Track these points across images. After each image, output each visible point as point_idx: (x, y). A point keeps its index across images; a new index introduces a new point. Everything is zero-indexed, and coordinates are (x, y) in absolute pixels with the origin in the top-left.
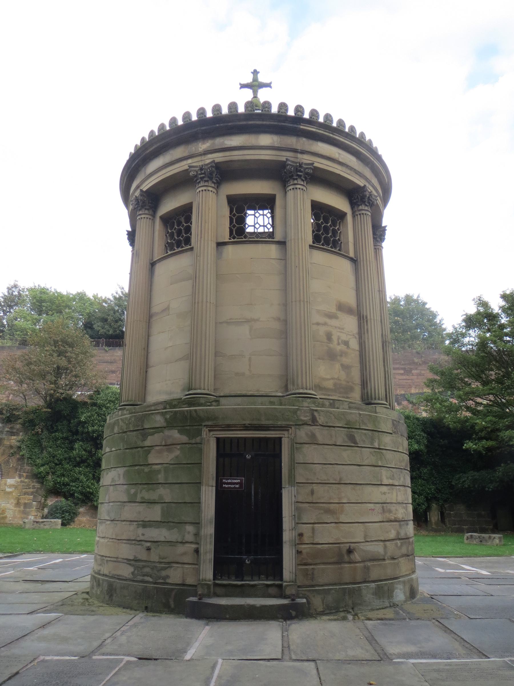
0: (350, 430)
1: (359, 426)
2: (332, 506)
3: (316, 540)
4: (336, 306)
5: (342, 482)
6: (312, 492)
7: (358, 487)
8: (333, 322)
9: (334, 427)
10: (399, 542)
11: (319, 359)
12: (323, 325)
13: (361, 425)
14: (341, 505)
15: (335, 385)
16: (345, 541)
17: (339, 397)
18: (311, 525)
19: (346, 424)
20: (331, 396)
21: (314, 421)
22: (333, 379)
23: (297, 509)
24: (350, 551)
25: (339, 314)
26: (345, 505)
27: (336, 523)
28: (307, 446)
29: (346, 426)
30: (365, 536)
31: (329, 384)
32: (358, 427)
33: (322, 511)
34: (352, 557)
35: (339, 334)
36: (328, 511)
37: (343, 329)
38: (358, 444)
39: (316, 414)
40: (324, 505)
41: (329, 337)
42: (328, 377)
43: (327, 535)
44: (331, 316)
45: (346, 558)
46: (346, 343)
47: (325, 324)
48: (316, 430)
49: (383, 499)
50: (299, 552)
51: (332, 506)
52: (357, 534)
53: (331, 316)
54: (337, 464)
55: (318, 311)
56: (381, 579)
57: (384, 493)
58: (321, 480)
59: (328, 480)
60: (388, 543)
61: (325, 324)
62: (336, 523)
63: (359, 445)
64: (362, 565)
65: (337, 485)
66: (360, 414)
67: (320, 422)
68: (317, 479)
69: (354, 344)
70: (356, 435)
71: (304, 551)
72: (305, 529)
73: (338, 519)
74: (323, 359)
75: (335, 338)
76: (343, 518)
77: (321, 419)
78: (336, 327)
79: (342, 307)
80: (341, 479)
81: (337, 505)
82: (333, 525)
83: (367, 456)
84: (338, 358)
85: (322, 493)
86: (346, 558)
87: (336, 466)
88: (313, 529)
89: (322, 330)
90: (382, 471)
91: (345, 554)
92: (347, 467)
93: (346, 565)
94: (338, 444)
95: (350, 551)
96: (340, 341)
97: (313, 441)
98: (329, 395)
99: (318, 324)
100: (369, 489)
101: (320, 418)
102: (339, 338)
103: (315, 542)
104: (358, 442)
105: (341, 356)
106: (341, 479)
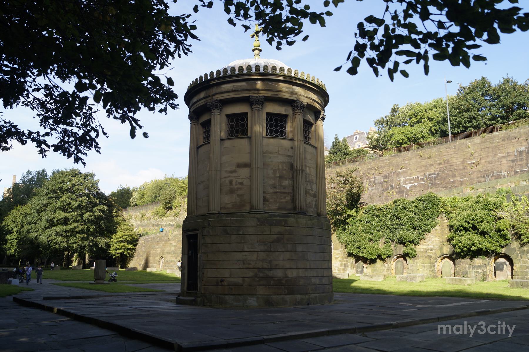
8: (234, 174)
24: (222, 281)
25: (238, 169)
31: (230, 206)
34: (223, 283)
41: (231, 182)
44: (232, 172)
45: (220, 284)
46: (241, 183)
47: (229, 177)
52: (226, 274)
53: (232, 172)
55: (226, 171)
57: (246, 255)
60: (246, 279)
61: (229, 177)
75: (234, 182)
79: (239, 166)
86: (220, 284)
89: (227, 180)
93: (220, 287)
95: (222, 281)
99: (225, 178)
102: (236, 181)
105: (237, 190)
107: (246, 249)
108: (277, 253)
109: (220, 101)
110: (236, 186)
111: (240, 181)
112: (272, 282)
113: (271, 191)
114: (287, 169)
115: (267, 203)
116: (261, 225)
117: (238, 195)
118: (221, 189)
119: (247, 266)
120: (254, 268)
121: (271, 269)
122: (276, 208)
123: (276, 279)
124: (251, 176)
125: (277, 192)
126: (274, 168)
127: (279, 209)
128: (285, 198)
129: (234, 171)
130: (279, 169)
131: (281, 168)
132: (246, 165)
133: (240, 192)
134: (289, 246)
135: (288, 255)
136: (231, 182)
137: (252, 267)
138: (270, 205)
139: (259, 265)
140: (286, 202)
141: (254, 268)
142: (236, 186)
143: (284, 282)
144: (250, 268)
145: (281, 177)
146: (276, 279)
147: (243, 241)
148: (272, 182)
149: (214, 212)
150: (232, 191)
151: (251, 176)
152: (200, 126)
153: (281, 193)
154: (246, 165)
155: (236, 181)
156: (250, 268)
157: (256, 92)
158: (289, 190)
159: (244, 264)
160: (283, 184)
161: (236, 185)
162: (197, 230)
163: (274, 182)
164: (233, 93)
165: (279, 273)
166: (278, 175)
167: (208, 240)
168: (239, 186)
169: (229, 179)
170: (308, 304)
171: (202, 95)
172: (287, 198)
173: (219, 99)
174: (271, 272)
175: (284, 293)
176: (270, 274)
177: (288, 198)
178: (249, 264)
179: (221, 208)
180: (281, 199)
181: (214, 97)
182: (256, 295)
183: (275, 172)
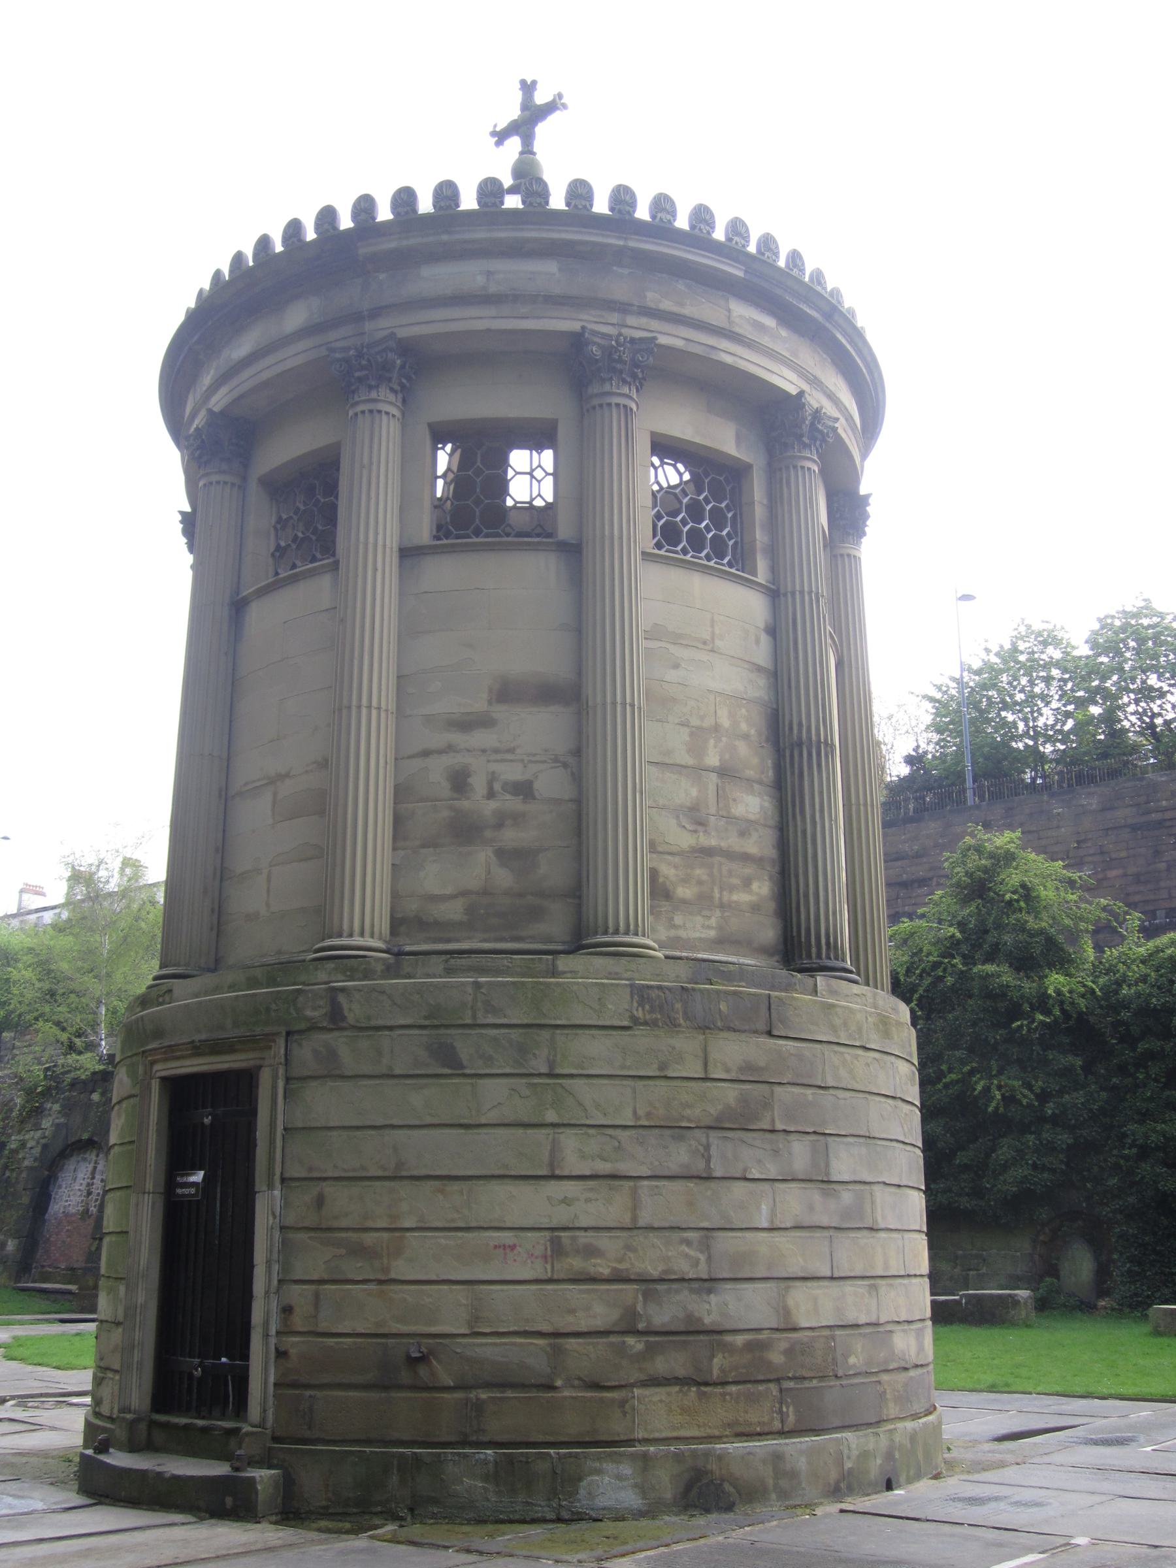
0: (442, 1031)
1: (474, 1017)
2: (369, 1238)
3: (323, 1326)
4: (490, 690)
5: (404, 1173)
6: (320, 1201)
7: (455, 1186)
8: (481, 738)
9: (390, 1028)
10: (635, 1344)
11: (423, 846)
12: (440, 752)
13: (480, 1014)
14: (397, 1234)
15: (470, 910)
16: (404, 1329)
17: (485, 940)
18: (314, 1287)
19: (426, 1018)
20: (458, 941)
21: (336, 1018)
22: (464, 893)
23: (284, 1242)
24: (414, 1362)
25: (500, 712)
26: (408, 1234)
27: (381, 1282)
28: (314, 1084)
29: (427, 1023)
30: (475, 1319)
31: (454, 911)
32: (468, 1021)
33: (343, 1251)
34: (423, 1371)
35: (494, 767)
36: (358, 1251)
37: (511, 751)
38: (463, 1067)
39: (342, 998)
40: (350, 1234)
41: (459, 781)
42: (449, 890)
43: (360, 1314)
44: (466, 724)
46: (524, 790)
47: (450, 749)
48: (339, 1041)
49: (561, 1216)
50: (281, 1354)
51: (369, 1238)
52: (449, 1316)
53: (466, 724)
54: (393, 1127)
56: (532, 1440)
57: (566, 1201)
58: (345, 1170)
59: (363, 1168)
61: (450, 749)
62: (381, 1282)
63: (468, 1071)
64: (459, 1395)
65: (387, 1184)
66: (477, 986)
67: (351, 1019)
68: (335, 1167)
69: (551, 784)
70: (458, 1045)
71: (293, 1352)
72: (298, 1295)
73: (386, 1270)
74: (436, 846)
75: (478, 783)
76: (401, 1269)
77: (354, 1011)
78: (484, 751)
79: (508, 692)
80: (400, 1165)
81: (385, 1235)
82: (372, 1286)
83: (497, 1096)
84: (488, 834)
85: (344, 1204)
86: (405, 1377)
87: (387, 1131)
88: (317, 1296)
90: (562, 1137)
91: (406, 1364)
92: (416, 1133)
94: (398, 1071)
96: (497, 787)
97: (331, 1071)
98: (449, 941)
99: (426, 753)
100: (500, 1190)
101: (350, 1010)
102: (492, 778)
103: (320, 1330)
104: (465, 1063)
105: (499, 826)
106: (400, 1165)
107: (572, 1163)
108: (739, 1190)
109: (406, 348)
110: (493, 805)
111: (512, 772)
112: (718, 1362)
113: (685, 840)
114: (753, 732)
115: (665, 906)
116: (653, 1024)
117: (505, 855)
118: (398, 820)
119: (576, 1263)
120: (618, 1278)
121: (709, 1284)
122: (712, 933)
123: (740, 1339)
124: (578, 752)
125: (707, 852)
126: (695, 722)
127: (722, 941)
128: (747, 883)
129: (483, 722)
130: (716, 728)
131: (726, 722)
132: (546, 693)
133: (511, 837)
134: (800, 1153)
135: (794, 1202)
136: (459, 781)
137: (606, 1272)
138: (678, 920)
139: (650, 1259)
140: (755, 908)
141: (618, 1278)
142: (493, 805)
143: (776, 1357)
144: (594, 1280)
145: (725, 772)
146: (740, 1339)
147: (551, 1116)
148: (685, 791)
149: (357, 941)
150: (465, 831)
151: (578, 752)
152: (253, 486)
153: (729, 855)
154: (546, 693)
155: (492, 778)
156: (594, 1280)
157: (614, 318)
158: (761, 844)
159: (557, 1250)
160: (739, 810)
161: (491, 794)
162: (261, 1042)
163: (694, 792)
164: (491, 311)
165: (745, 1308)
166: (713, 760)
167: (324, 1103)
168: (512, 803)
169: (448, 760)
170: (889, 1486)
171: (296, 317)
172: (755, 886)
173: (402, 333)
174: (713, 1298)
175: (777, 1425)
176: (712, 1309)
177: (763, 888)
178: (591, 1252)
179: (397, 924)
180: (732, 889)
181: (368, 326)
182: (630, 1442)
183: (699, 736)
